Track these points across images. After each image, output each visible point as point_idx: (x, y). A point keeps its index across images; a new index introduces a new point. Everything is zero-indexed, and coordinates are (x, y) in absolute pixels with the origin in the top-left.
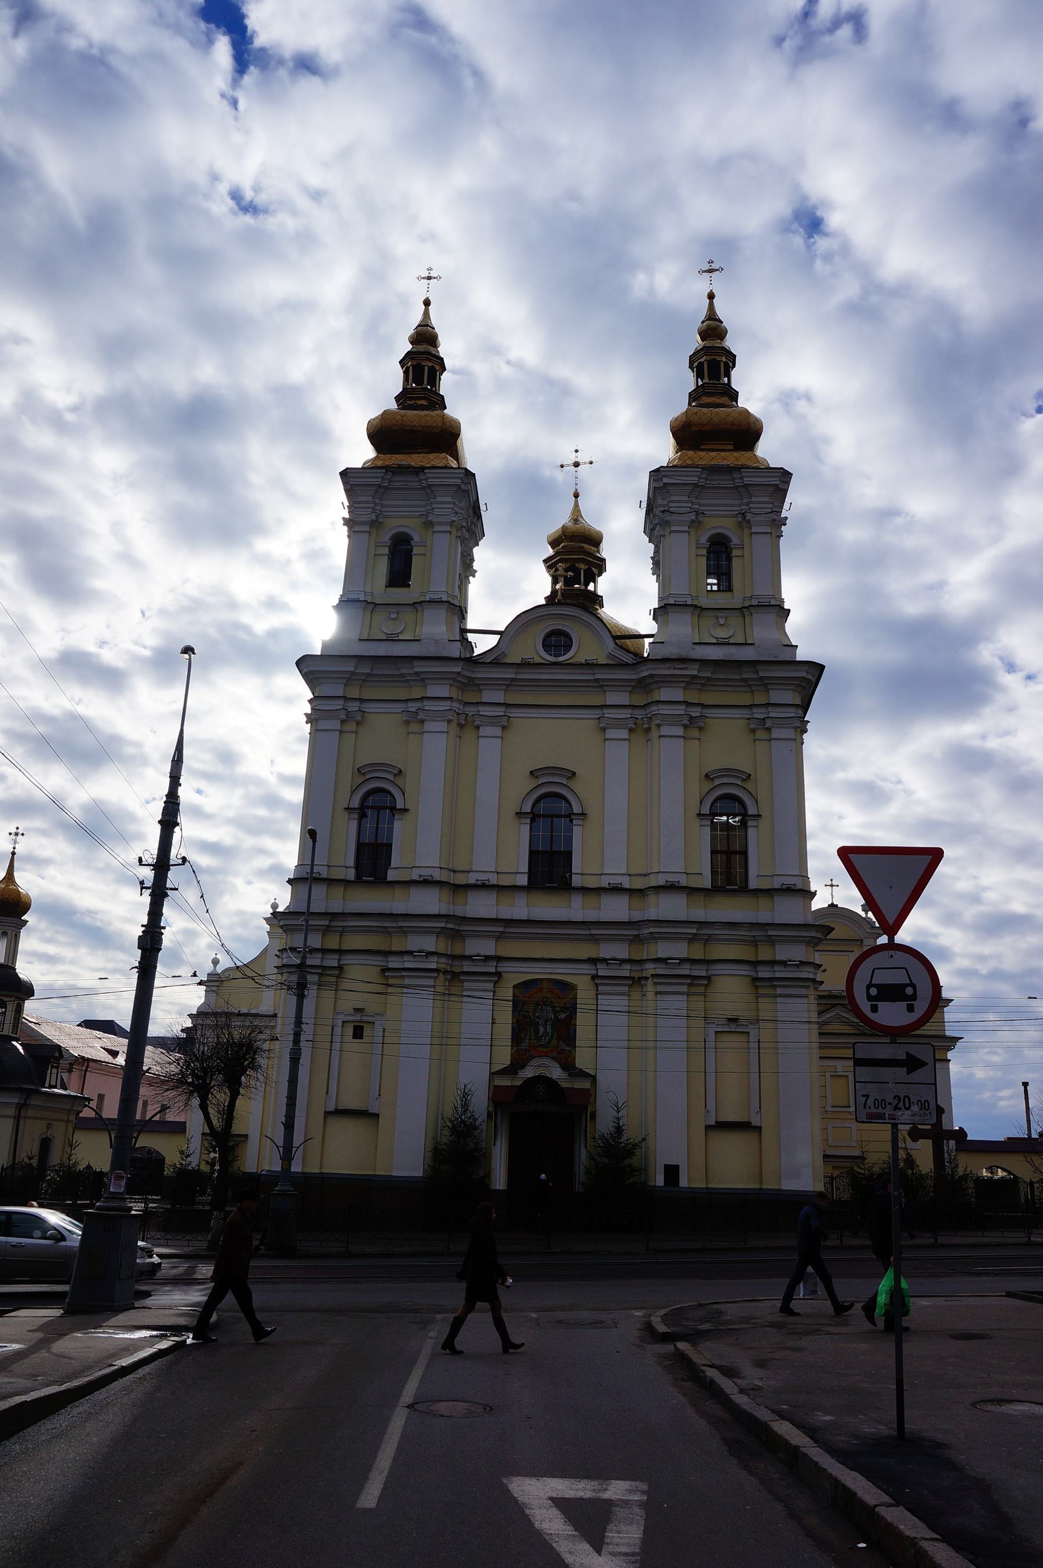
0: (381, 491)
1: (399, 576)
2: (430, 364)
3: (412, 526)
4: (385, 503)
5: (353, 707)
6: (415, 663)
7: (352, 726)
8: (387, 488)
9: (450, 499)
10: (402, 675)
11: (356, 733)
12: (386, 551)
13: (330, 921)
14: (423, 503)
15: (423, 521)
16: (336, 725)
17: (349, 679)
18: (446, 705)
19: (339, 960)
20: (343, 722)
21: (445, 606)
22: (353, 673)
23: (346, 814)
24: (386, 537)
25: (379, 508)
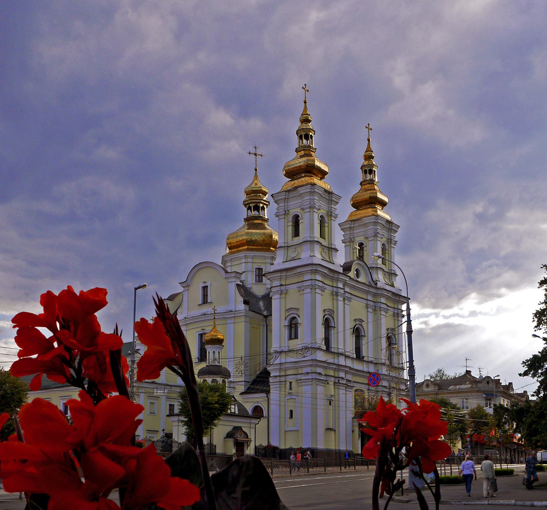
0: (286, 200)
1: (296, 233)
3: (297, 211)
4: (289, 204)
5: (283, 288)
6: (298, 269)
7: (283, 296)
8: (288, 198)
9: (308, 198)
10: (295, 273)
11: (285, 298)
12: (291, 224)
13: (280, 366)
14: (300, 201)
15: (300, 208)
16: (278, 296)
17: (280, 278)
18: (309, 283)
19: (285, 379)
20: (281, 294)
21: (309, 242)
22: (281, 276)
23: (284, 327)
24: (290, 218)
25: (287, 207)
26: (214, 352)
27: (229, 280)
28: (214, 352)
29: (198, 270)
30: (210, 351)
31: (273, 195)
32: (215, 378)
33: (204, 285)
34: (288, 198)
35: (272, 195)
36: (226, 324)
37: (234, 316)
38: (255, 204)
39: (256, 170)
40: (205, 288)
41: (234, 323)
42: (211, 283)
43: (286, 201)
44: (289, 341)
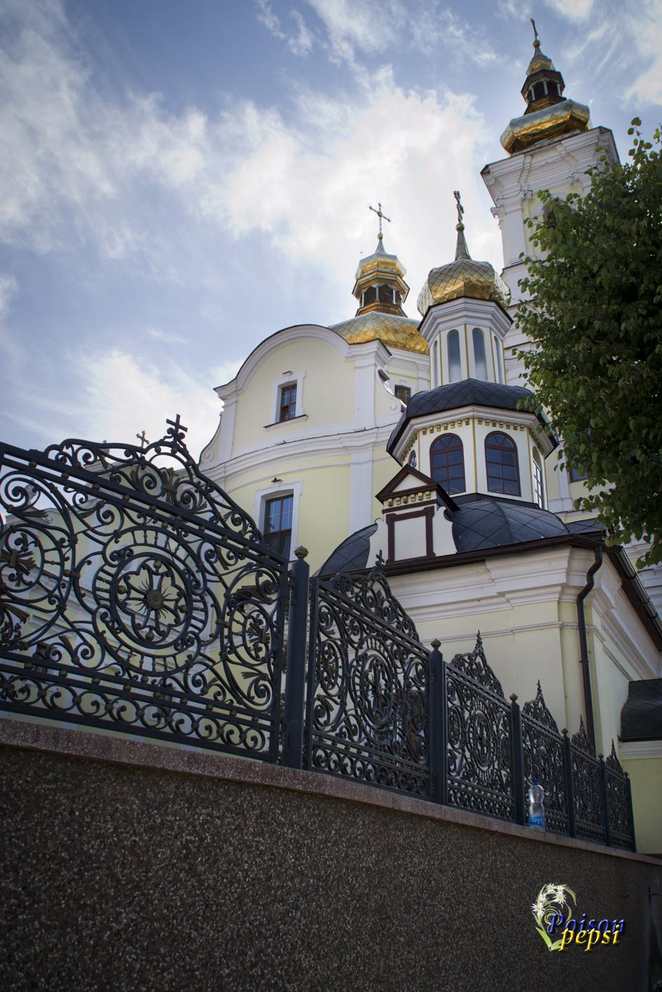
2: (548, 80)
26: (478, 334)
27: (359, 363)
28: (478, 334)
29: (271, 349)
30: (461, 330)
31: (490, 167)
32: (504, 430)
33: (285, 380)
34: (529, 172)
35: (487, 166)
36: (349, 465)
37: (374, 440)
38: (382, 284)
39: (381, 238)
40: (288, 390)
41: (373, 461)
42: (306, 372)
43: (524, 178)
44: (571, 484)
